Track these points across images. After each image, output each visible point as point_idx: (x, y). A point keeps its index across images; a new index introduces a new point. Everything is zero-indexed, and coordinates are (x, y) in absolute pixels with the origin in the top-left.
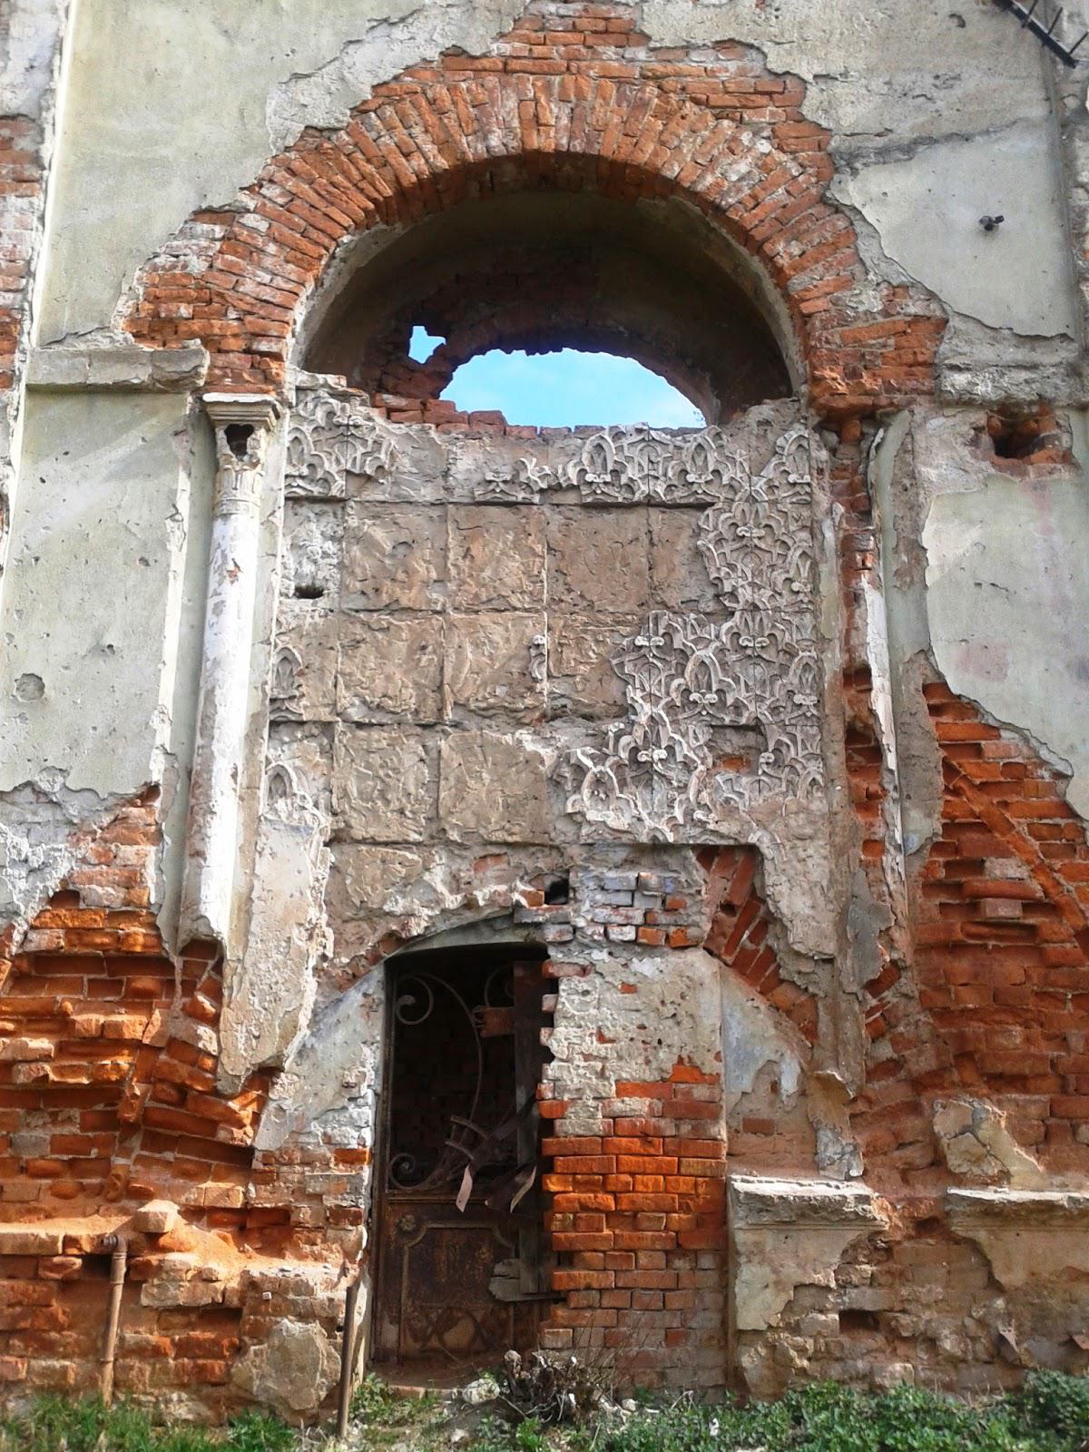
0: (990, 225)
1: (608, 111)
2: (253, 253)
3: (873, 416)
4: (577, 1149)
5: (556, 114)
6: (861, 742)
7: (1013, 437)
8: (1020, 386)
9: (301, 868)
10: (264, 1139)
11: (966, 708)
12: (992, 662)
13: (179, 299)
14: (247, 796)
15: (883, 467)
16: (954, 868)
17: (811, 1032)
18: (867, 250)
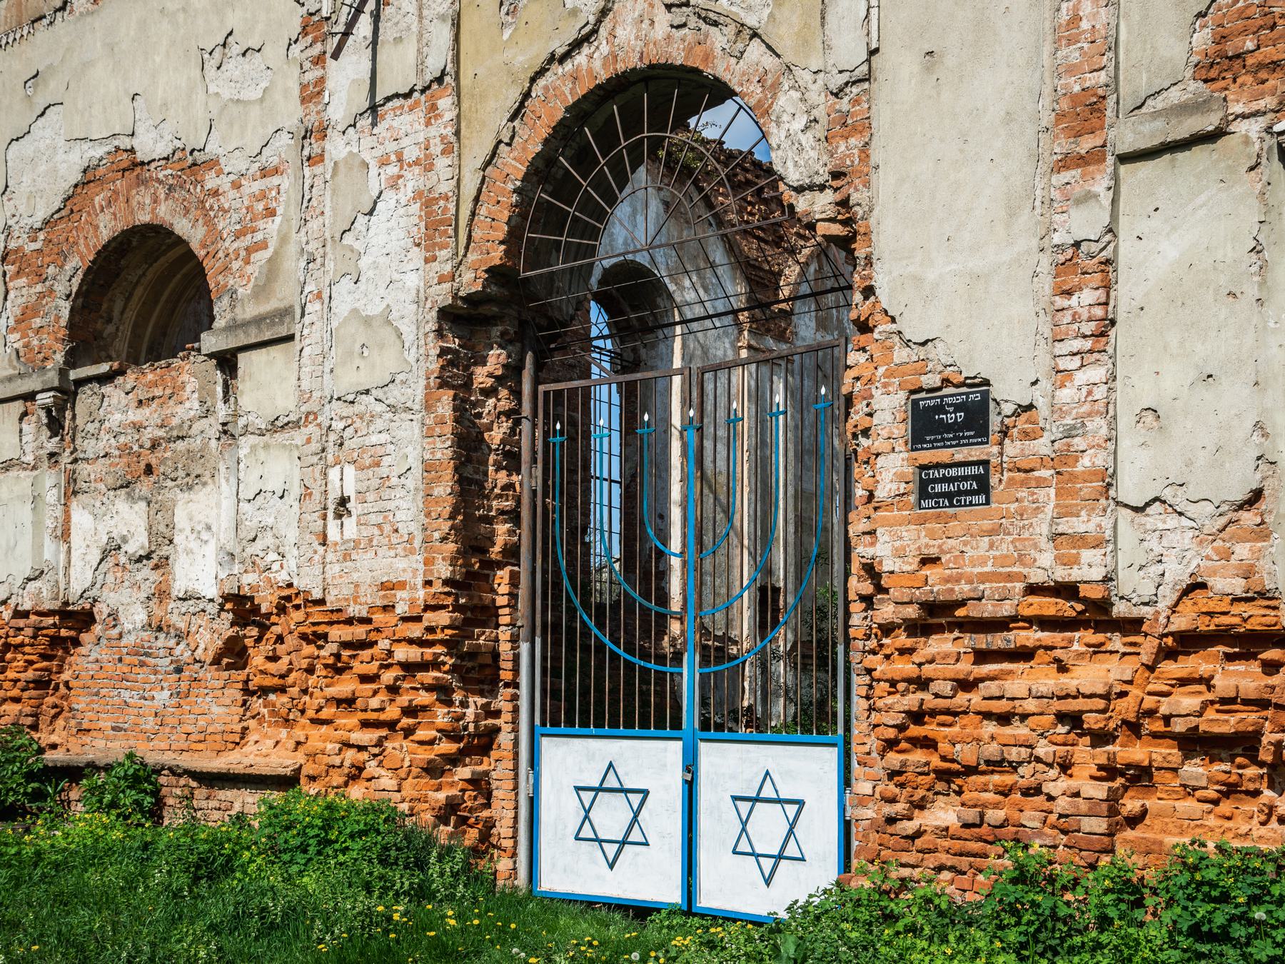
13: (1244, 32)
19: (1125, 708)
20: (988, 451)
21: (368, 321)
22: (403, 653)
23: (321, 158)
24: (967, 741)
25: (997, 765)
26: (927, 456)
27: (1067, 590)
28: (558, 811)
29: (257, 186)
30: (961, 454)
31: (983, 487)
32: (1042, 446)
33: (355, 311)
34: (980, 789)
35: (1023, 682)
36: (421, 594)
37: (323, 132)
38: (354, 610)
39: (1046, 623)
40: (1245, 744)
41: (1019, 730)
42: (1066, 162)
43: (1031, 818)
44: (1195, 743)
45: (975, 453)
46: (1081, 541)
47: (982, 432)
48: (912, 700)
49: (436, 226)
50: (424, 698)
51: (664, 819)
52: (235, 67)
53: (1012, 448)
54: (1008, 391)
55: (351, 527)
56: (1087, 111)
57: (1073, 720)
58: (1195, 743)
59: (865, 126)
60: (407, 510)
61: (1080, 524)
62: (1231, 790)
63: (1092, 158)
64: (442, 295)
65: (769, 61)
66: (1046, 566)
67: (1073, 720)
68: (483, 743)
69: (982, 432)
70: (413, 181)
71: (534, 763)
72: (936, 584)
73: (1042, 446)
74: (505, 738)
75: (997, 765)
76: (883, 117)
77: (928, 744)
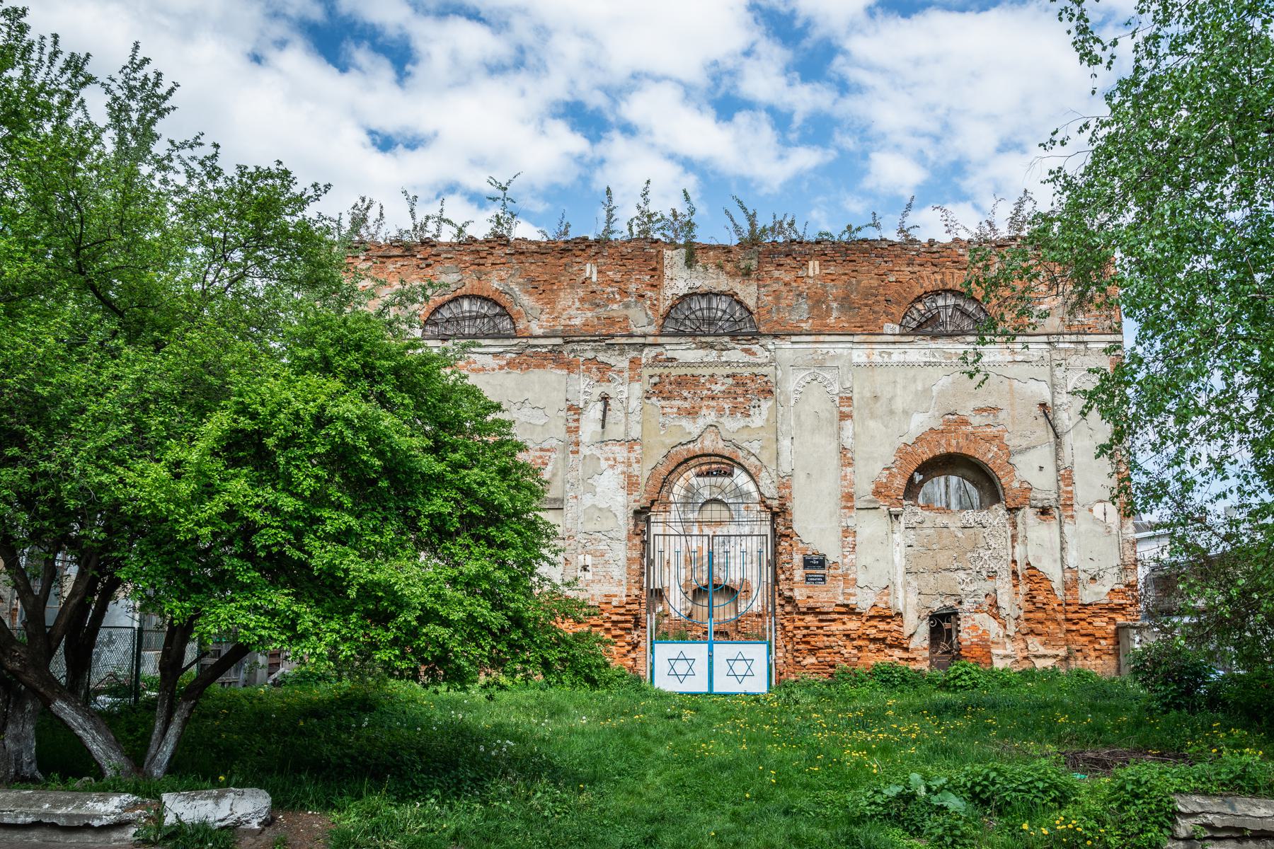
0: (1041, 468)
1: (963, 442)
2: (895, 476)
3: (1018, 509)
4: (966, 647)
5: (954, 442)
6: (1014, 573)
7: (1044, 511)
8: (1046, 504)
9: (913, 599)
10: (911, 646)
11: (1034, 568)
12: (1039, 559)
14: (904, 587)
15: (1019, 520)
16: (1031, 598)
17: (1005, 627)
18: (1017, 473)
19: (860, 632)
20: (825, 571)
21: (600, 509)
22: (615, 618)
23: (577, 452)
24: (819, 641)
25: (827, 647)
26: (809, 571)
27: (847, 606)
28: (661, 667)
29: (538, 454)
30: (818, 572)
31: (824, 580)
32: (840, 571)
33: (594, 506)
34: (822, 654)
35: (835, 627)
36: (625, 599)
37: (577, 444)
38: (591, 603)
39: (839, 613)
40: (884, 639)
41: (832, 639)
42: (845, 507)
43: (837, 659)
44: (874, 640)
45: (822, 572)
46: (850, 594)
47: (823, 567)
48: (805, 632)
49: (631, 484)
50: (619, 632)
51: (701, 667)
52: (525, 410)
53: (832, 571)
54: (831, 558)
55: (589, 576)
56: (849, 497)
57: (848, 636)
58: (874, 640)
59: (789, 487)
60: (618, 572)
61: (851, 591)
62: (879, 650)
63: (852, 507)
64: (637, 506)
65: (757, 463)
66: (841, 600)
67: (848, 636)
68: (635, 646)
69: (823, 567)
70: (620, 468)
71: (652, 652)
72: (811, 603)
73: (840, 571)
74: (642, 644)
75: (827, 647)
76: (795, 486)
77: (808, 643)
